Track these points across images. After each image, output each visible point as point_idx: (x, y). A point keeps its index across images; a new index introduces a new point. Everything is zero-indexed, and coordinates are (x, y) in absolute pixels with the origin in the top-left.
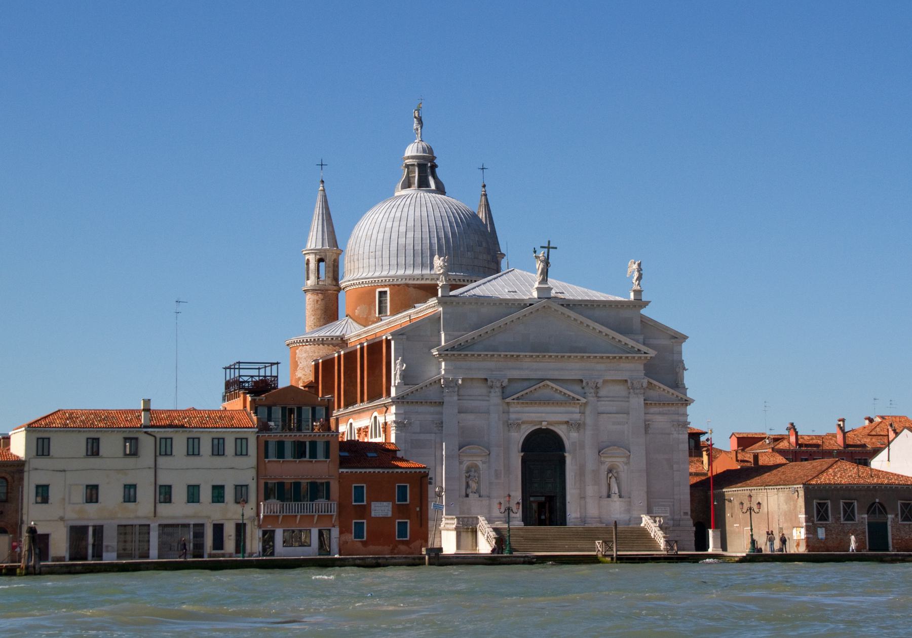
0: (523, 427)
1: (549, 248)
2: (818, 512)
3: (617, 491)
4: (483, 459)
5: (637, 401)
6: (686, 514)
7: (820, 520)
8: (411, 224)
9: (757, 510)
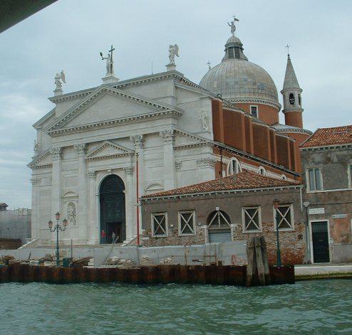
0: (98, 175)
5: (168, 148)
9: (63, 227)
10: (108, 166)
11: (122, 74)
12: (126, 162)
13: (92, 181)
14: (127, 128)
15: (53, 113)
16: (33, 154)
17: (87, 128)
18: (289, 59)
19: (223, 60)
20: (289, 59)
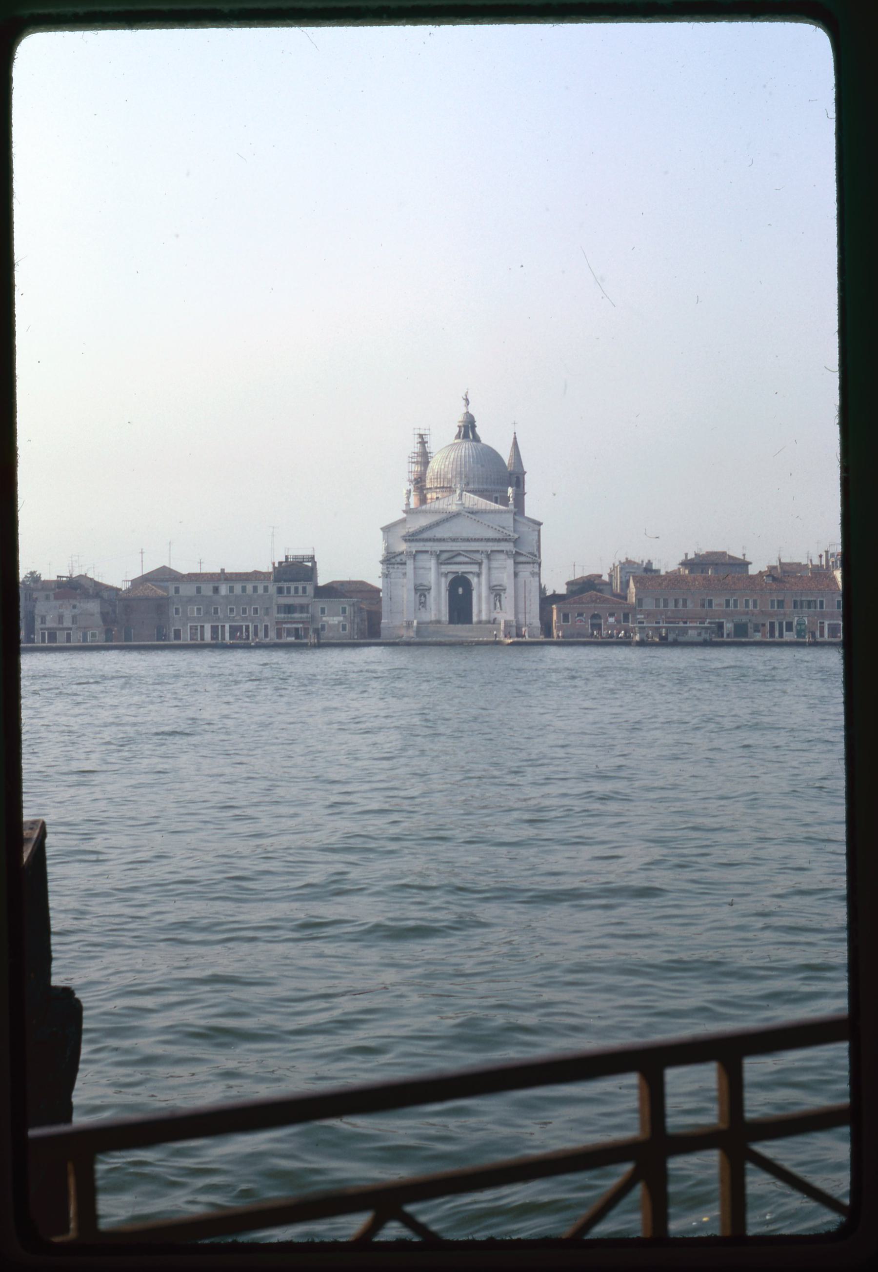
5: (510, 562)
8: (452, 460)
12: (474, 568)
13: (443, 580)
14: (477, 544)
15: (403, 521)
18: (515, 438)
19: (458, 436)
20: (515, 438)
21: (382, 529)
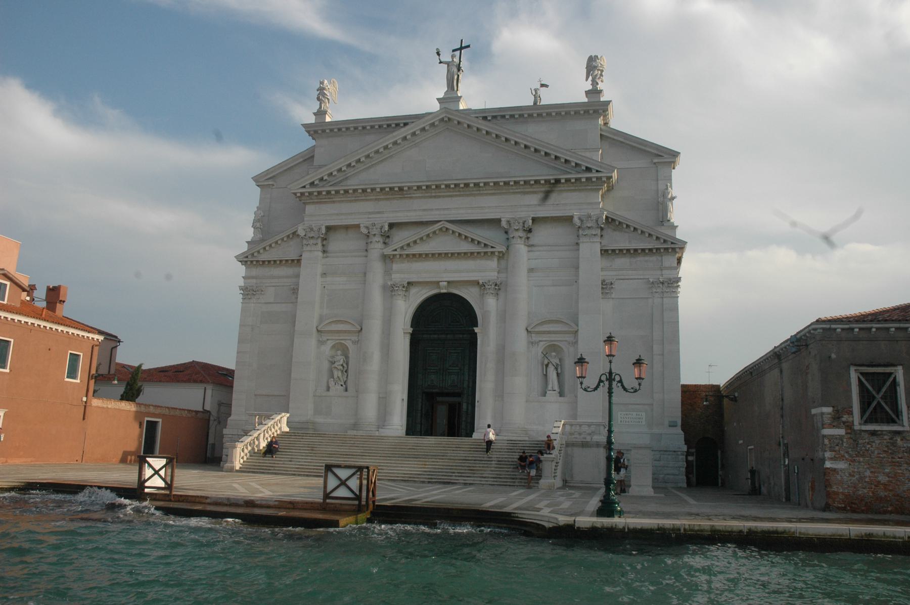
0: (414, 290)
1: (461, 49)
2: (866, 399)
3: (556, 387)
4: (355, 338)
5: (590, 249)
6: (672, 425)
7: (868, 421)
9: (630, 383)
10: (445, 275)
11: (474, 96)
12: (487, 270)
15: (308, 158)
16: (249, 233)
17: (399, 192)
21: (256, 179)
